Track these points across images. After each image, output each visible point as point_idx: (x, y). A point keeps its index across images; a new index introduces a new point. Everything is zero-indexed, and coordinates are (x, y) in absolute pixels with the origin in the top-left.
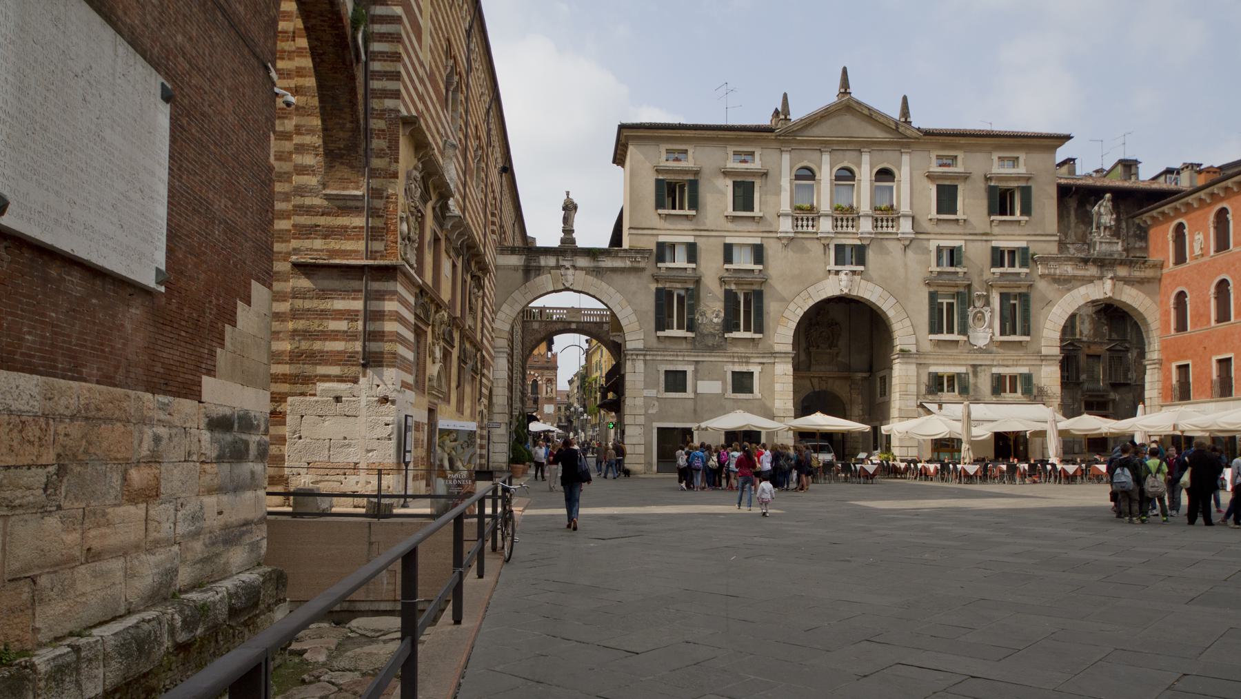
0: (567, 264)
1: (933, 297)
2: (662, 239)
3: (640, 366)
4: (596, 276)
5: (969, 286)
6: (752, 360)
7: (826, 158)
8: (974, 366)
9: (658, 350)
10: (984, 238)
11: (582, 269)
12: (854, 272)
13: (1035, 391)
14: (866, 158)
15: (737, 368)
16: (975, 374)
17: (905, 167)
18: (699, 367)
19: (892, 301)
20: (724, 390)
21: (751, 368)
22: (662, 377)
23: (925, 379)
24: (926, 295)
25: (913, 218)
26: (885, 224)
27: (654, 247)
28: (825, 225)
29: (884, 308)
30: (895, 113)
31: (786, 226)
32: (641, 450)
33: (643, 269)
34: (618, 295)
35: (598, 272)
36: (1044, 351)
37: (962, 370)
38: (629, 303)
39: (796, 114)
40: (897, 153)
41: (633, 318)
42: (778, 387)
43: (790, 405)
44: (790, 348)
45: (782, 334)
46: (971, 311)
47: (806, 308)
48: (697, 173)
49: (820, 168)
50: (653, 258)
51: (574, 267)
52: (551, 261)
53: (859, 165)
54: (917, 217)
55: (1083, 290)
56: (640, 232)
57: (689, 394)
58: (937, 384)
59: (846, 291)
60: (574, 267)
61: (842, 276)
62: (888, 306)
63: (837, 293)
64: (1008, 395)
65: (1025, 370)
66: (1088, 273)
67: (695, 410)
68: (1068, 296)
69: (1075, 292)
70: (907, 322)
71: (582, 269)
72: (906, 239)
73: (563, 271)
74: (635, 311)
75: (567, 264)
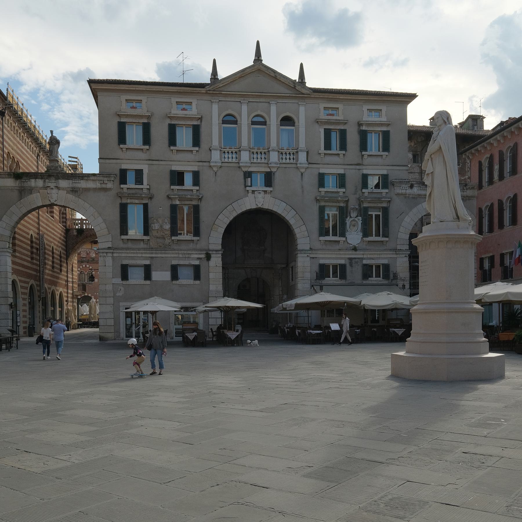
0: (52, 185)
1: (322, 210)
2: (124, 167)
3: (109, 260)
5: (347, 202)
6: (193, 256)
8: (351, 259)
9: (122, 249)
10: (358, 167)
11: (63, 189)
12: (265, 192)
13: (391, 276)
17: (302, 113)
19: (293, 212)
23: (316, 268)
25: (308, 153)
26: (288, 157)
27: (118, 173)
31: (216, 156)
32: (111, 322)
33: (110, 189)
35: (74, 191)
36: (399, 247)
37: (342, 262)
39: (222, 74)
41: (103, 225)
42: (211, 275)
43: (220, 288)
44: (220, 247)
46: (348, 221)
47: (231, 218)
48: (149, 117)
49: (241, 116)
50: (118, 180)
51: (57, 188)
52: (40, 183)
53: (269, 114)
54: (309, 152)
56: (107, 161)
58: (323, 271)
59: (260, 206)
60: (57, 188)
62: (290, 217)
63: (254, 207)
64: (374, 280)
65: (385, 262)
68: (415, 210)
70: (304, 228)
71: (63, 189)
72: (303, 168)
73: (49, 191)
74: (105, 221)
75: (52, 185)
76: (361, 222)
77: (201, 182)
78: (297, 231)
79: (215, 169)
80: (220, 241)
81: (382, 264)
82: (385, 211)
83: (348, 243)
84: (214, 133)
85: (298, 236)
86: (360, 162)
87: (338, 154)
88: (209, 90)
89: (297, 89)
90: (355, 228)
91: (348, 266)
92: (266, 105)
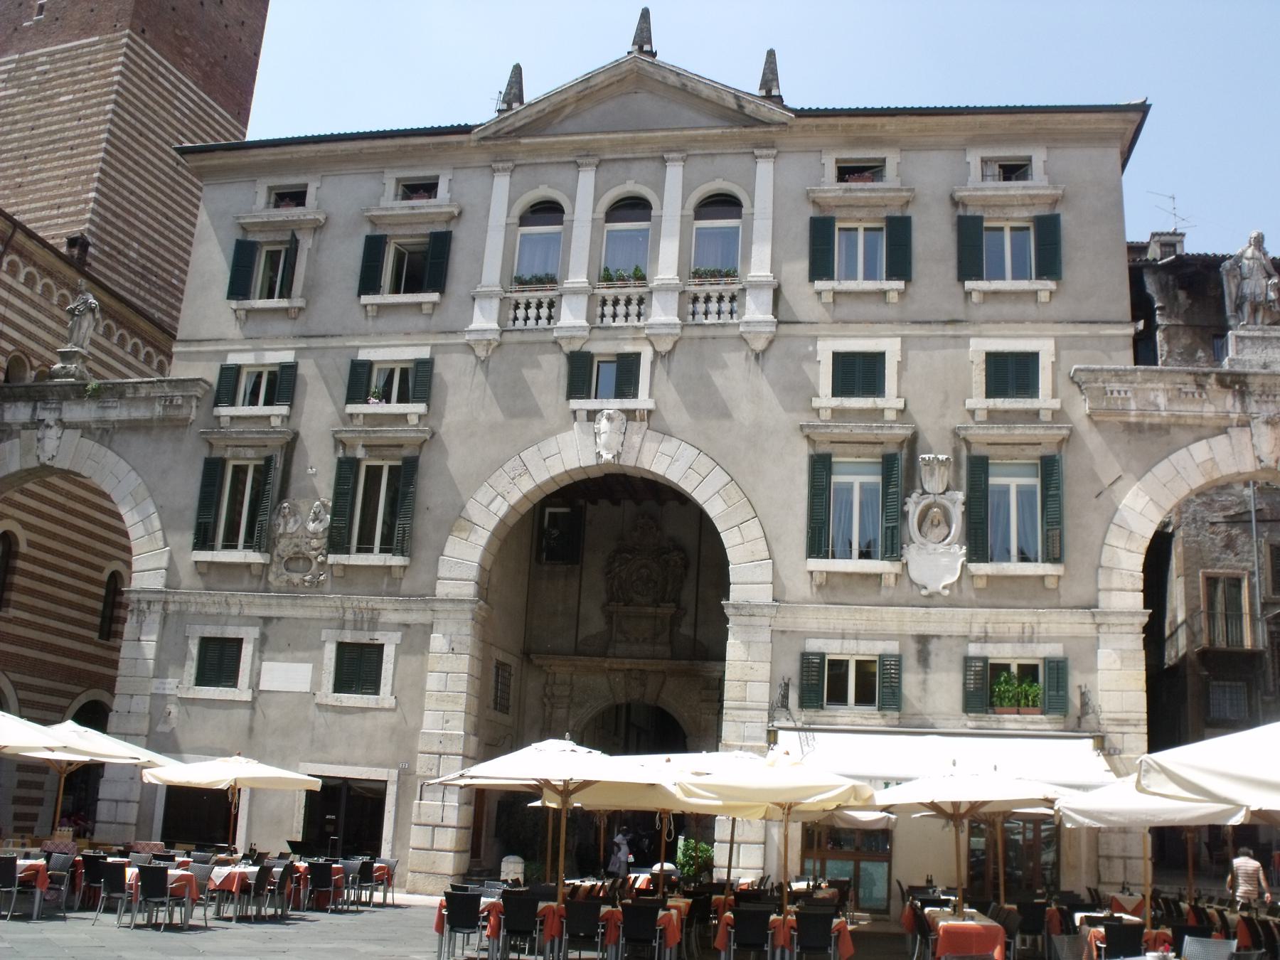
1: (820, 467)
4: (100, 441)
5: (912, 442)
7: (587, 179)
8: (923, 640)
10: (950, 330)
14: (674, 174)
15: (349, 637)
16: (924, 659)
18: (270, 631)
19: (719, 477)
20: (316, 683)
21: (380, 637)
22: (194, 649)
23: (791, 668)
24: (804, 464)
25: (777, 293)
28: (572, 316)
29: (699, 496)
30: (751, 84)
33: (184, 423)
34: (133, 474)
37: (892, 647)
38: (152, 492)
40: (747, 160)
43: (457, 727)
45: (461, 561)
46: (913, 507)
47: (515, 497)
49: (573, 199)
53: (659, 188)
55: (1200, 450)
57: (242, 692)
59: (607, 456)
61: (603, 425)
63: (591, 461)
66: (1209, 410)
67: (251, 730)
69: (1180, 456)
70: (754, 529)
76: (962, 508)
77: (435, 391)
78: (729, 539)
79: (481, 353)
80: (473, 572)
81: (1047, 661)
82: (1049, 468)
83: (912, 582)
84: (487, 252)
85: (731, 555)
86: (959, 311)
87: (883, 293)
88: (484, 139)
89: (753, 120)
90: (943, 530)
91: (910, 661)
92: (653, 166)
